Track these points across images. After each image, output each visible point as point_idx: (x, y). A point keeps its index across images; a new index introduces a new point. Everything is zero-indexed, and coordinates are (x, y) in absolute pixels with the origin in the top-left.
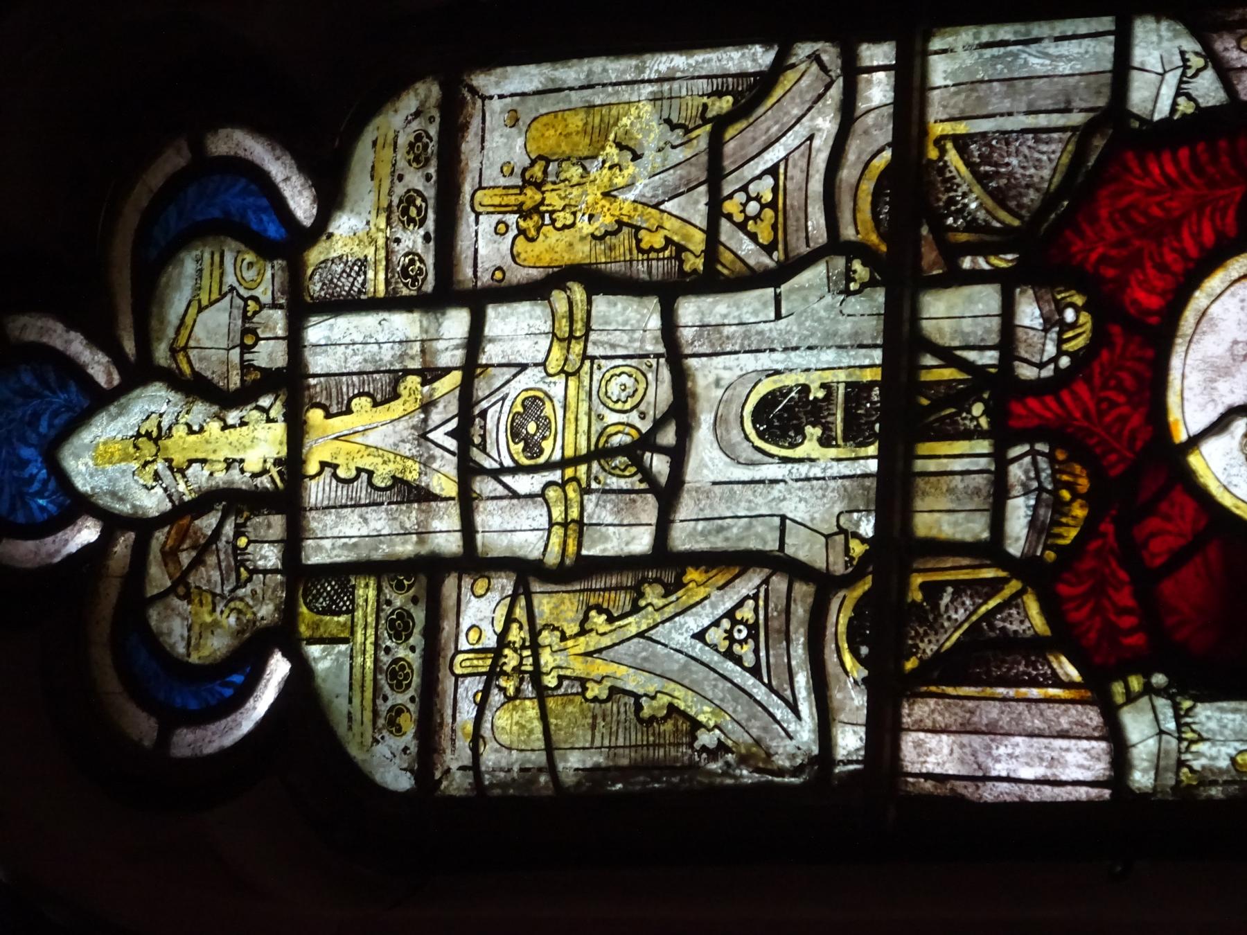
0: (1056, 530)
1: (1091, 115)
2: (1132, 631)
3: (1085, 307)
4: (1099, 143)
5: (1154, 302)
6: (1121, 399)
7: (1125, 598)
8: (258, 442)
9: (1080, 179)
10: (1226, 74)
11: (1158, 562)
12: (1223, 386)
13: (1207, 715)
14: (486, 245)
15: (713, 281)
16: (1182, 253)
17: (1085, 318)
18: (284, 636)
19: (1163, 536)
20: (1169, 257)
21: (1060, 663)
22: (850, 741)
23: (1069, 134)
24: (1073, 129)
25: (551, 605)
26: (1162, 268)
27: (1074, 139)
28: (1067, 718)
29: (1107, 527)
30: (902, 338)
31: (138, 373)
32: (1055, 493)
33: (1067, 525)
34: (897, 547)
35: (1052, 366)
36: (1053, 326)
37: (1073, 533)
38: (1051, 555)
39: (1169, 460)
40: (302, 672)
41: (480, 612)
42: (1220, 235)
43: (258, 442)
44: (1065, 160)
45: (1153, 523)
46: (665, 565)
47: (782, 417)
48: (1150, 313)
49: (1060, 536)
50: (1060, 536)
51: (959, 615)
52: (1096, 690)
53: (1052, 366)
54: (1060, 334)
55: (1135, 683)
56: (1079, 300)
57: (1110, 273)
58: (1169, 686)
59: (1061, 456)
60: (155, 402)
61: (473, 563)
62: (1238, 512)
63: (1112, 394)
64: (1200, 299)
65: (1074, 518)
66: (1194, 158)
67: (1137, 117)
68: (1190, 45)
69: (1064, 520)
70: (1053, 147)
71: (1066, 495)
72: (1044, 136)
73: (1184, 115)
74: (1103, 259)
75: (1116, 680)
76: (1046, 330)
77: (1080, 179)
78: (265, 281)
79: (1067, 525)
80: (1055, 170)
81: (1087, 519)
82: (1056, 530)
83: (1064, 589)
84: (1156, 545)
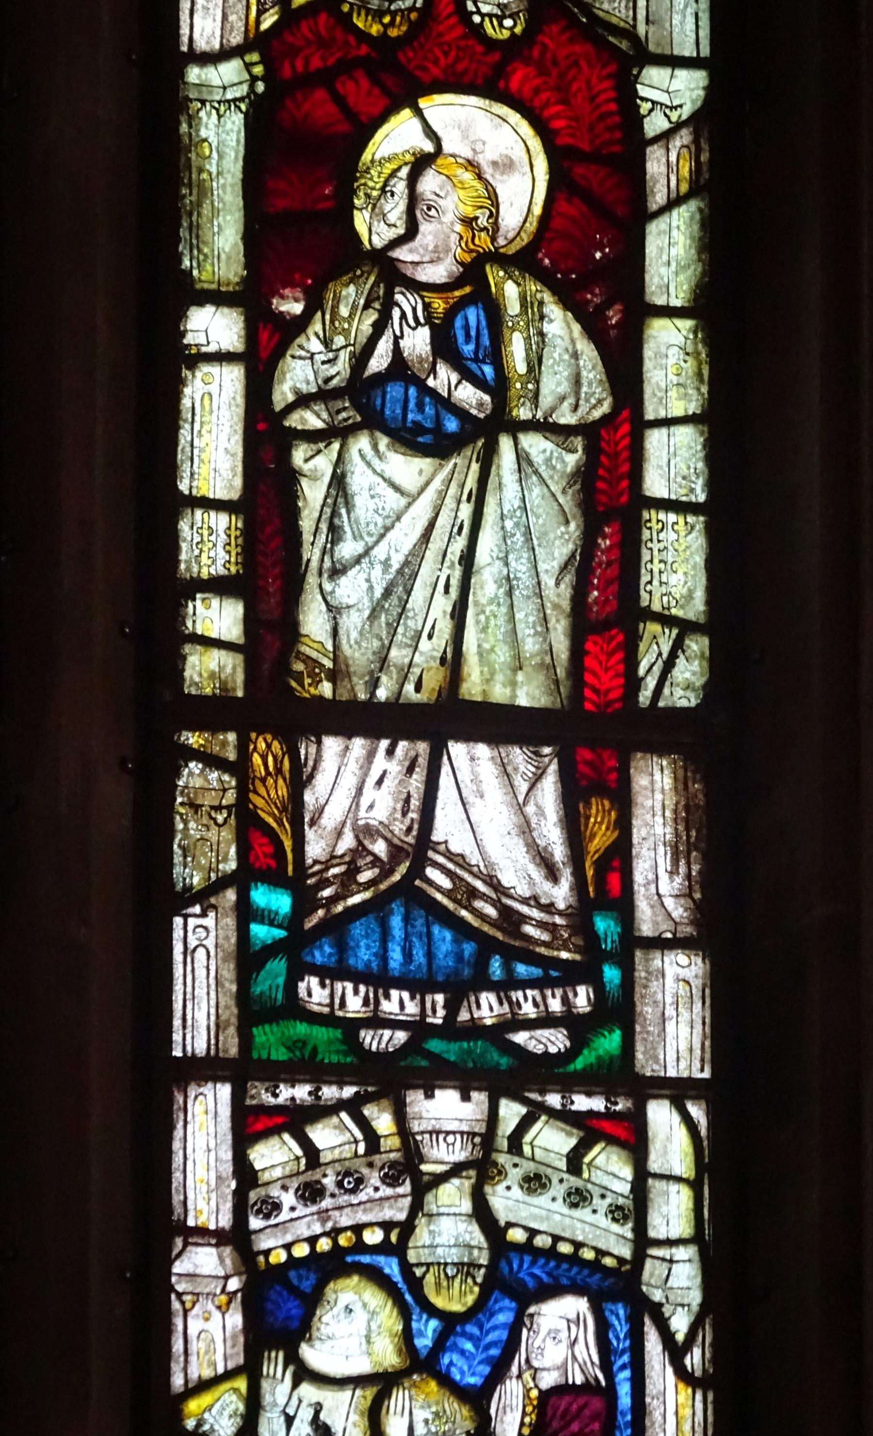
0: (363, 13)
1: (643, 39)
2: (293, 67)
3: (513, 34)
4: (624, 45)
5: (514, 84)
6: (450, 60)
7: (316, 63)
9: (600, 31)
10: (665, 137)
11: (339, 86)
12: (457, 133)
16: (547, 105)
17: (506, 34)
19: (357, 90)
20: (544, 96)
21: (273, 15)
23: (631, 23)
24: (634, 26)
26: (537, 91)
27: (627, 26)
29: (364, 50)
32: (388, 11)
33: (366, 20)
35: (474, 9)
36: (502, 11)
37: (360, 25)
38: (346, 8)
39: (406, 95)
42: (557, 132)
44: (614, 20)
45: (365, 83)
48: (507, 82)
49: (359, 15)
50: (359, 15)
53: (474, 9)
54: (496, 16)
56: (518, 30)
57: (536, 53)
58: (255, 94)
59: (414, 16)
62: (371, 144)
63: (453, 53)
64: (514, 117)
65: (371, 26)
66: (610, 114)
67: (640, 72)
68: (686, 112)
69: (370, 18)
70: (623, 11)
71: (387, 20)
72: (631, 4)
73: (639, 107)
74: (545, 47)
75: (261, 55)
76: (499, 5)
77: (600, 31)
79: (366, 20)
80: (608, 12)
81: (369, 35)
82: (363, 13)
83: (323, 17)
84: (350, 86)
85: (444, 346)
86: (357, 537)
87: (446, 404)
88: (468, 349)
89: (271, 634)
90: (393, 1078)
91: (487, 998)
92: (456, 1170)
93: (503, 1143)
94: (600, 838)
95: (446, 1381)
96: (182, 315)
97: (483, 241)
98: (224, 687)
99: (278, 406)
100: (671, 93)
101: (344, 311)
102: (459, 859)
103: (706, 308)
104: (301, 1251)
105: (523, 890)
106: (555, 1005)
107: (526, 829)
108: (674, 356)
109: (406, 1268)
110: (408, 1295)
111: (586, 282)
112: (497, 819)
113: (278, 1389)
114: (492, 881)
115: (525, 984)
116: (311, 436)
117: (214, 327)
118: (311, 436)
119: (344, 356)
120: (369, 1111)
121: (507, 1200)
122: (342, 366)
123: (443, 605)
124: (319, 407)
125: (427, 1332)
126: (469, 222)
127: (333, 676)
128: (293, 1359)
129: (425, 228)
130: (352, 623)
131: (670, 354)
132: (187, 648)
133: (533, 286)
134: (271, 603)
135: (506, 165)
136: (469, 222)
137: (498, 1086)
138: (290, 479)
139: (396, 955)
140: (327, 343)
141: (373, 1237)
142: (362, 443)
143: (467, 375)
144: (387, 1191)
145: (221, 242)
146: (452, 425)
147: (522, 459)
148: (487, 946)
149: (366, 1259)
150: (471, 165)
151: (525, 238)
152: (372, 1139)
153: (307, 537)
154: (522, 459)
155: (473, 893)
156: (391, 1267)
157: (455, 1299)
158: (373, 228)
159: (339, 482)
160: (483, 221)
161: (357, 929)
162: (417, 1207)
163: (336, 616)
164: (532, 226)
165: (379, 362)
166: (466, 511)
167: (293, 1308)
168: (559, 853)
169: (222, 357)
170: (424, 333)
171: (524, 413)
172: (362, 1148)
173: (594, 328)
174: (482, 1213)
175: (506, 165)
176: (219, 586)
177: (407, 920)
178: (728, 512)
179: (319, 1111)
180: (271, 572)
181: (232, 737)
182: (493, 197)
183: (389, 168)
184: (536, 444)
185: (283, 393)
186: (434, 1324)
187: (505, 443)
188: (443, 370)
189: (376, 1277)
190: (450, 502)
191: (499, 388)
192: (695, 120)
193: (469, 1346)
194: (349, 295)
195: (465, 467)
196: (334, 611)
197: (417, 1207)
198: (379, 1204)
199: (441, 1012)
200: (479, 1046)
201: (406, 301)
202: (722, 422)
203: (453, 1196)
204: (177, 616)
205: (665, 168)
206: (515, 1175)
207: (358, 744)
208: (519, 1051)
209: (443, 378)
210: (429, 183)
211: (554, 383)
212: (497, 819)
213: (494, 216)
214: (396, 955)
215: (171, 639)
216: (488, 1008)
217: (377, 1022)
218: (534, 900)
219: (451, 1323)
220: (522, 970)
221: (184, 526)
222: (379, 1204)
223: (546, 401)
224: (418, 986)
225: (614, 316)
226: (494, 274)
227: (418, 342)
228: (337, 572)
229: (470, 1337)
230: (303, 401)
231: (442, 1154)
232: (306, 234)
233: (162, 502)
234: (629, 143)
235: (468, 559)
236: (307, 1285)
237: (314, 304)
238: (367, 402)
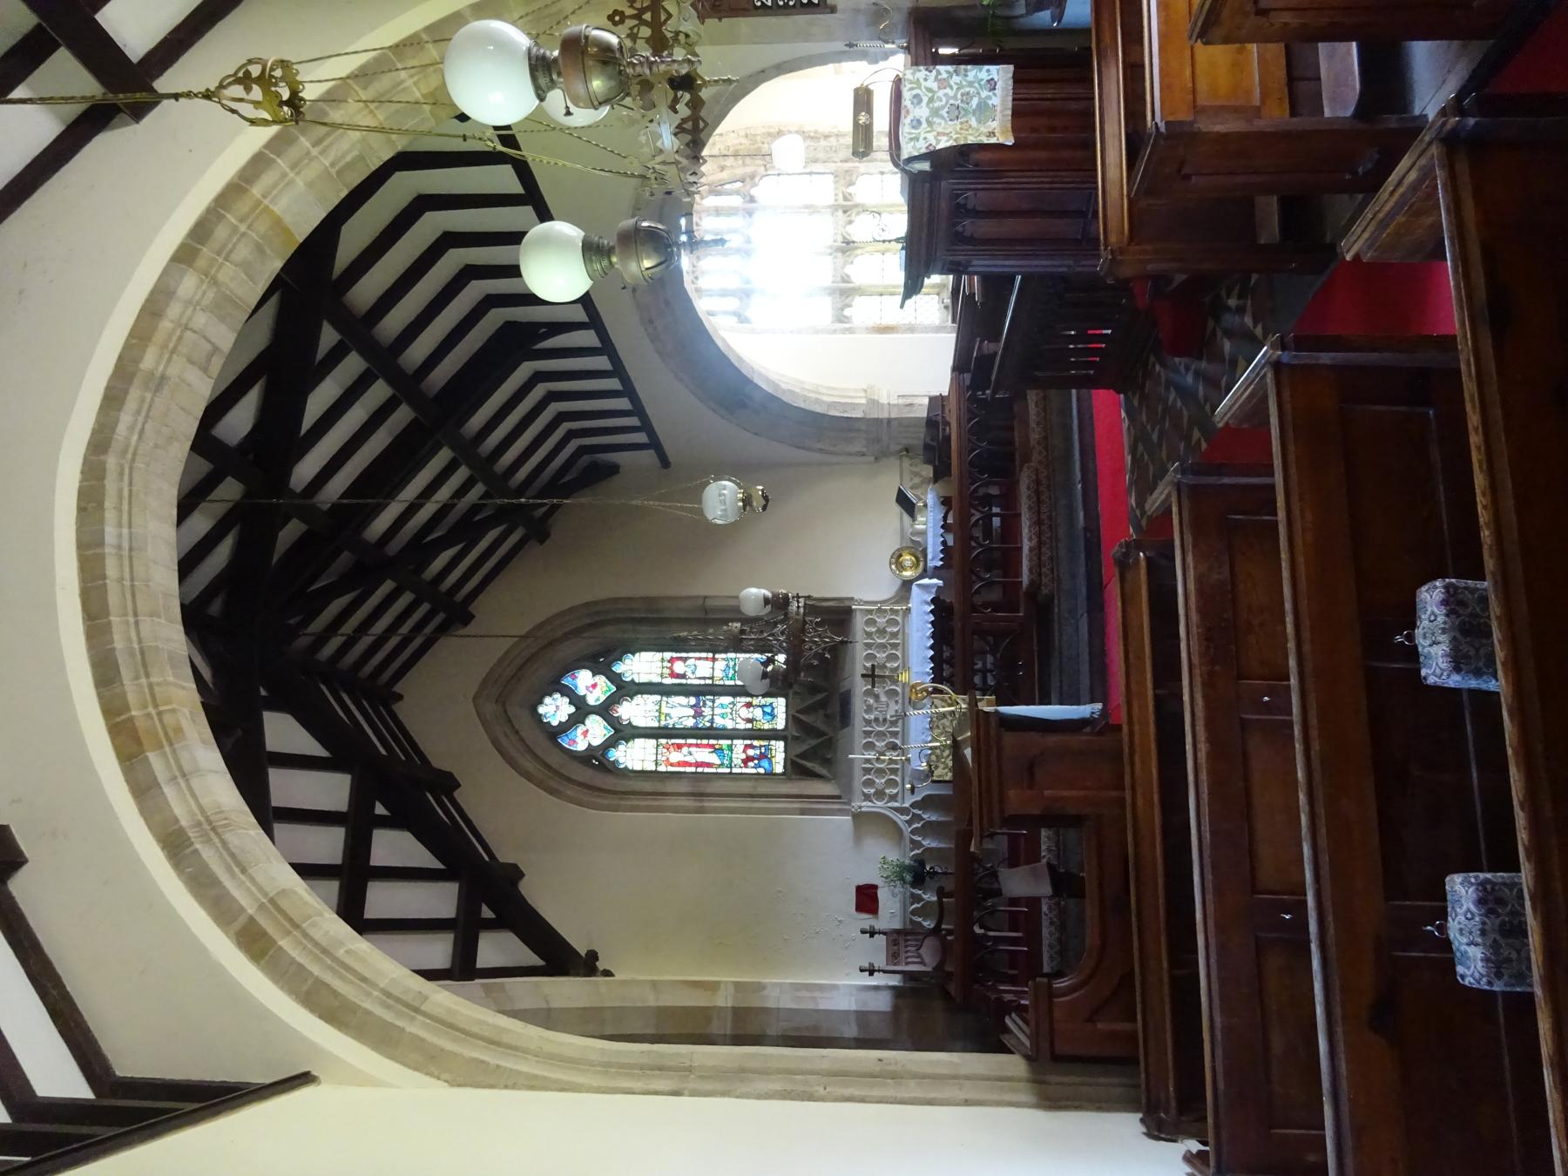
232: (683, 676)
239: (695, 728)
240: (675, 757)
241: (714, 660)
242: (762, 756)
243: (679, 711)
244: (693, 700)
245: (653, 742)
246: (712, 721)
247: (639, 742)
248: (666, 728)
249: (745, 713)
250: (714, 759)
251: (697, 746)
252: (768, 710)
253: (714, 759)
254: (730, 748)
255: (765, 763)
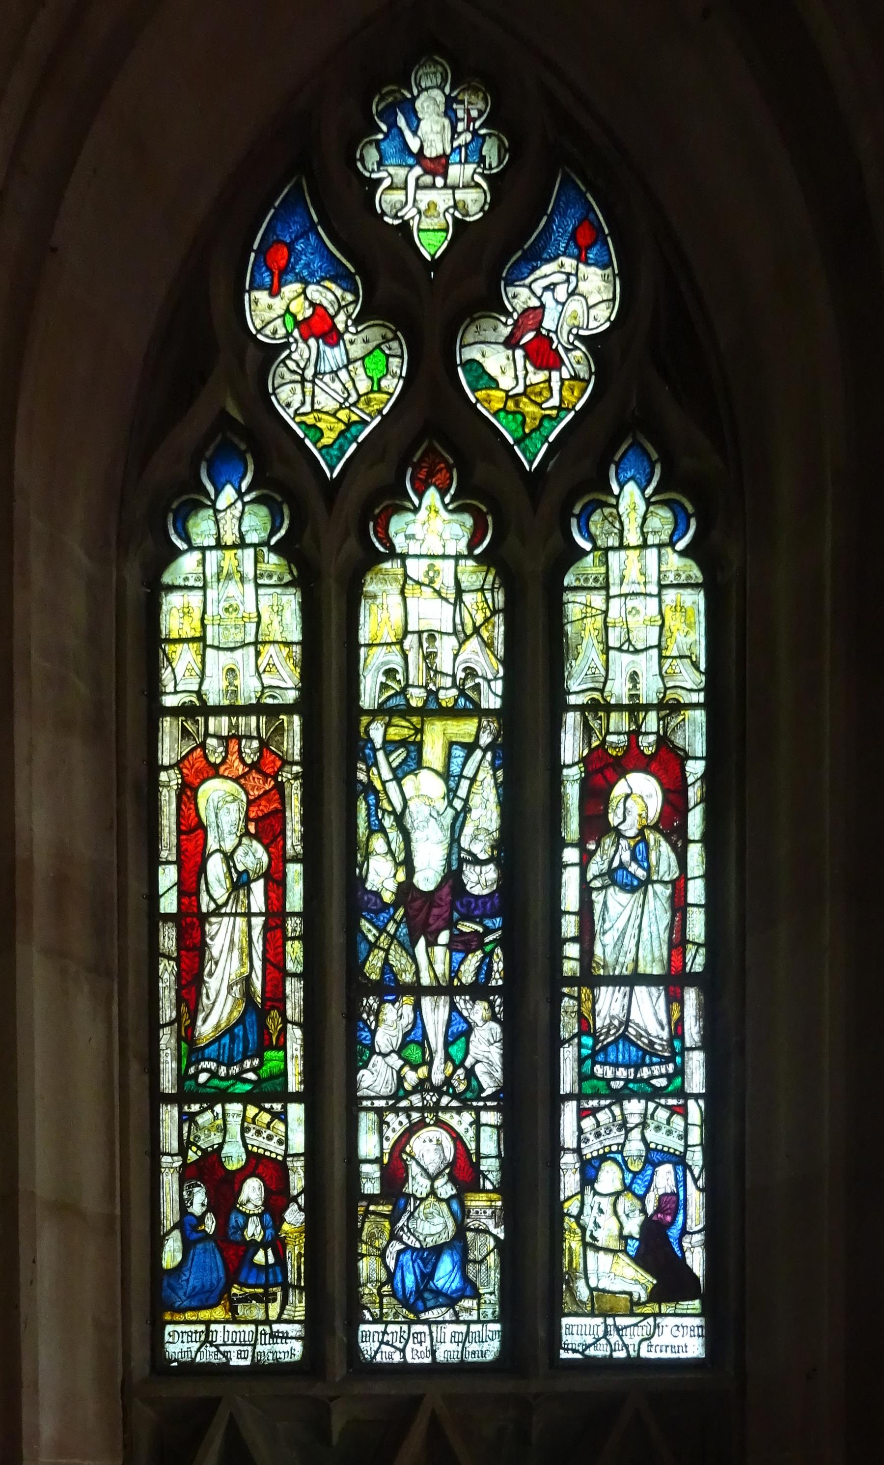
4: (682, 753)
8: (633, 537)
10: (694, 783)
13: (576, 786)
14: (670, 596)
15: (661, 657)
18: (595, 548)
22: (572, 700)
25: (600, 619)
28: (577, 753)
30: (647, 707)
31: (648, 502)
34: (609, 708)
39: (623, 774)
40: (585, 553)
41: (597, 600)
43: (633, 537)
46: (607, 649)
47: (634, 677)
51: (594, 724)
52: (583, 760)
55: (583, 769)
60: (642, 507)
61: (608, 598)
68: (699, 775)
78: (665, 538)
85: (634, 858)
86: (610, 921)
87: (634, 876)
88: (640, 858)
89: (587, 955)
90: (619, 1097)
91: (645, 1069)
92: (636, 1126)
93: (649, 1116)
94: (676, 1016)
95: (634, 1194)
96: (562, 852)
97: (644, 822)
98: (574, 973)
99: (588, 880)
100: (695, 769)
101: (606, 847)
102: (637, 1025)
103: (707, 839)
104: (595, 1154)
105: (655, 1034)
106: (664, 1071)
107: (656, 1014)
108: (696, 856)
109: (623, 1157)
110: (623, 1166)
111: (671, 834)
112: (648, 1011)
113: (589, 1198)
114: (646, 1031)
115: (655, 1064)
116: (598, 889)
117: (571, 855)
118: (598, 889)
119: (606, 862)
120: (613, 1108)
121: (650, 1135)
122: (606, 866)
123: (634, 942)
124: (599, 879)
125: (629, 1177)
126: (640, 815)
127: (604, 967)
128: (593, 1188)
129: (628, 818)
130: (609, 950)
131: (695, 854)
132: (564, 961)
133: (658, 835)
134: (586, 945)
135: (650, 796)
136: (640, 815)
137: (649, 1097)
138: (591, 903)
139: (620, 1057)
140: (602, 858)
141: (614, 1148)
142: (611, 890)
143: (640, 866)
144: (618, 1133)
145: (572, 828)
146: (635, 883)
147: (655, 893)
148: (645, 1052)
149: (612, 1155)
150: (641, 797)
151: (655, 820)
152: (614, 1116)
153: (596, 922)
154: (655, 893)
155: (641, 1036)
156: (619, 1158)
157: (636, 1167)
158: (614, 819)
159: (605, 903)
160: (644, 815)
161: (610, 1049)
162: (626, 1138)
163: (604, 948)
164: (657, 816)
165: (616, 864)
166: (640, 910)
167: (593, 1172)
168: (665, 1021)
169: (572, 865)
170: (628, 852)
171: (655, 878)
172: (611, 1120)
173: (674, 848)
174: (644, 1139)
175: (650, 796)
176: (573, 940)
177: (624, 1045)
178: (712, 907)
179: (599, 1109)
180: (587, 935)
181: (576, 988)
182: (646, 806)
183: (618, 799)
184: (658, 887)
185: (589, 876)
186: (631, 1175)
187: (650, 887)
188: (633, 864)
189: (615, 1160)
190: (635, 908)
191: (648, 870)
192: (702, 777)
193: (639, 1182)
194: (608, 841)
195: (639, 895)
196: (604, 946)
197: (626, 1138)
198: (615, 1137)
199: (633, 1075)
200: (643, 1085)
201: (623, 843)
202: (711, 877)
203: (636, 1134)
204: (561, 950)
205: (694, 794)
206: (652, 1126)
207: (611, 988)
208: (653, 1086)
209: (633, 867)
210: (629, 803)
211: (663, 867)
212: (648, 1011)
213: (647, 813)
214: (620, 1057)
215: (558, 958)
216: (645, 1073)
217: (615, 1079)
218: (657, 1037)
219: (635, 1174)
220: (655, 1059)
221: (563, 921)
222: (615, 1137)
223: (661, 873)
224: (627, 1067)
225: (680, 844)
226: (647, 832)
227: (626, 856)
228: (604, 933)
229: (640, 1179)
230: (595, 877)
231: (633, 1120)
232: (596, 824)
233: (556, 913)
234: (684, 787)
235: (640, 927)
236: (597, 1165)
237: (598, 845)
238: (613, 876)
239: (358, 899)
240: (221, 803)
241: (673, 982)
242: (234, 1252)
243: (433, 818)
244: (481, 880)
245: (286, 681)
246: (391, 988)
247: (285, 614)
248: (356, 748)
249: (429, 1149)
250: (219, 1009)
251: (275, 914)
252: (445, 1274)
253: (219, 1009)
254: (268, 1093)
255: (210, 1266)
